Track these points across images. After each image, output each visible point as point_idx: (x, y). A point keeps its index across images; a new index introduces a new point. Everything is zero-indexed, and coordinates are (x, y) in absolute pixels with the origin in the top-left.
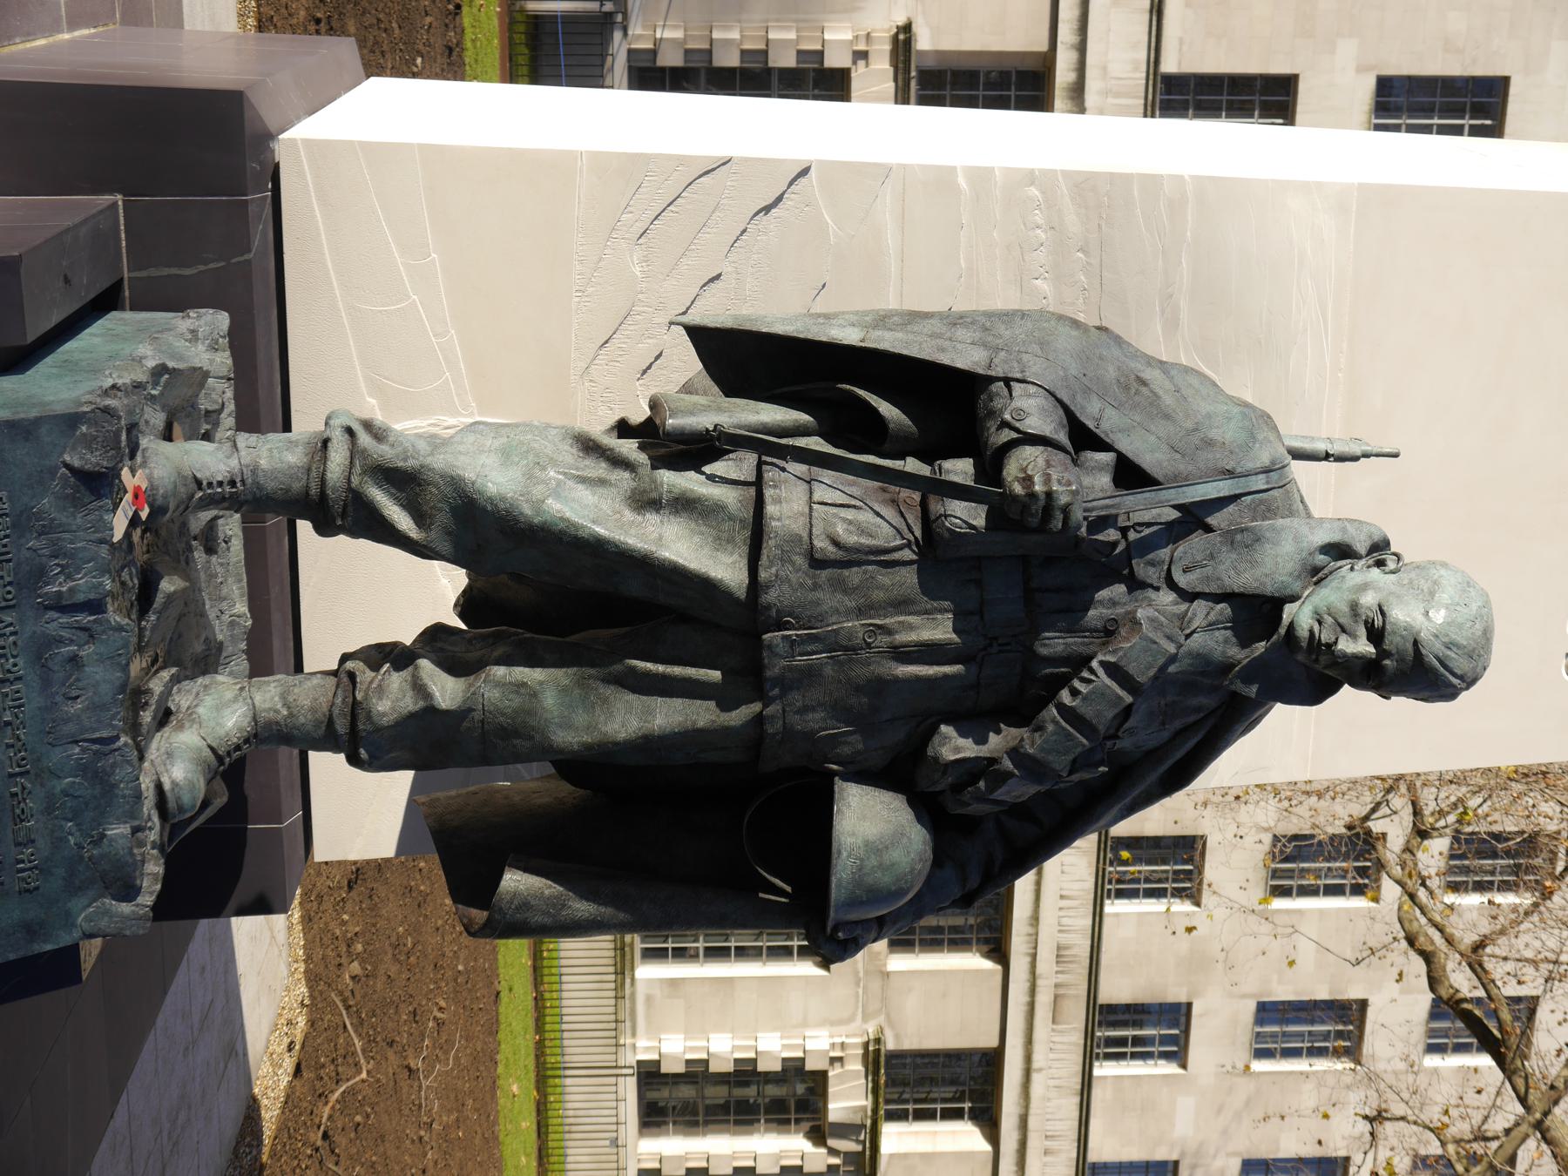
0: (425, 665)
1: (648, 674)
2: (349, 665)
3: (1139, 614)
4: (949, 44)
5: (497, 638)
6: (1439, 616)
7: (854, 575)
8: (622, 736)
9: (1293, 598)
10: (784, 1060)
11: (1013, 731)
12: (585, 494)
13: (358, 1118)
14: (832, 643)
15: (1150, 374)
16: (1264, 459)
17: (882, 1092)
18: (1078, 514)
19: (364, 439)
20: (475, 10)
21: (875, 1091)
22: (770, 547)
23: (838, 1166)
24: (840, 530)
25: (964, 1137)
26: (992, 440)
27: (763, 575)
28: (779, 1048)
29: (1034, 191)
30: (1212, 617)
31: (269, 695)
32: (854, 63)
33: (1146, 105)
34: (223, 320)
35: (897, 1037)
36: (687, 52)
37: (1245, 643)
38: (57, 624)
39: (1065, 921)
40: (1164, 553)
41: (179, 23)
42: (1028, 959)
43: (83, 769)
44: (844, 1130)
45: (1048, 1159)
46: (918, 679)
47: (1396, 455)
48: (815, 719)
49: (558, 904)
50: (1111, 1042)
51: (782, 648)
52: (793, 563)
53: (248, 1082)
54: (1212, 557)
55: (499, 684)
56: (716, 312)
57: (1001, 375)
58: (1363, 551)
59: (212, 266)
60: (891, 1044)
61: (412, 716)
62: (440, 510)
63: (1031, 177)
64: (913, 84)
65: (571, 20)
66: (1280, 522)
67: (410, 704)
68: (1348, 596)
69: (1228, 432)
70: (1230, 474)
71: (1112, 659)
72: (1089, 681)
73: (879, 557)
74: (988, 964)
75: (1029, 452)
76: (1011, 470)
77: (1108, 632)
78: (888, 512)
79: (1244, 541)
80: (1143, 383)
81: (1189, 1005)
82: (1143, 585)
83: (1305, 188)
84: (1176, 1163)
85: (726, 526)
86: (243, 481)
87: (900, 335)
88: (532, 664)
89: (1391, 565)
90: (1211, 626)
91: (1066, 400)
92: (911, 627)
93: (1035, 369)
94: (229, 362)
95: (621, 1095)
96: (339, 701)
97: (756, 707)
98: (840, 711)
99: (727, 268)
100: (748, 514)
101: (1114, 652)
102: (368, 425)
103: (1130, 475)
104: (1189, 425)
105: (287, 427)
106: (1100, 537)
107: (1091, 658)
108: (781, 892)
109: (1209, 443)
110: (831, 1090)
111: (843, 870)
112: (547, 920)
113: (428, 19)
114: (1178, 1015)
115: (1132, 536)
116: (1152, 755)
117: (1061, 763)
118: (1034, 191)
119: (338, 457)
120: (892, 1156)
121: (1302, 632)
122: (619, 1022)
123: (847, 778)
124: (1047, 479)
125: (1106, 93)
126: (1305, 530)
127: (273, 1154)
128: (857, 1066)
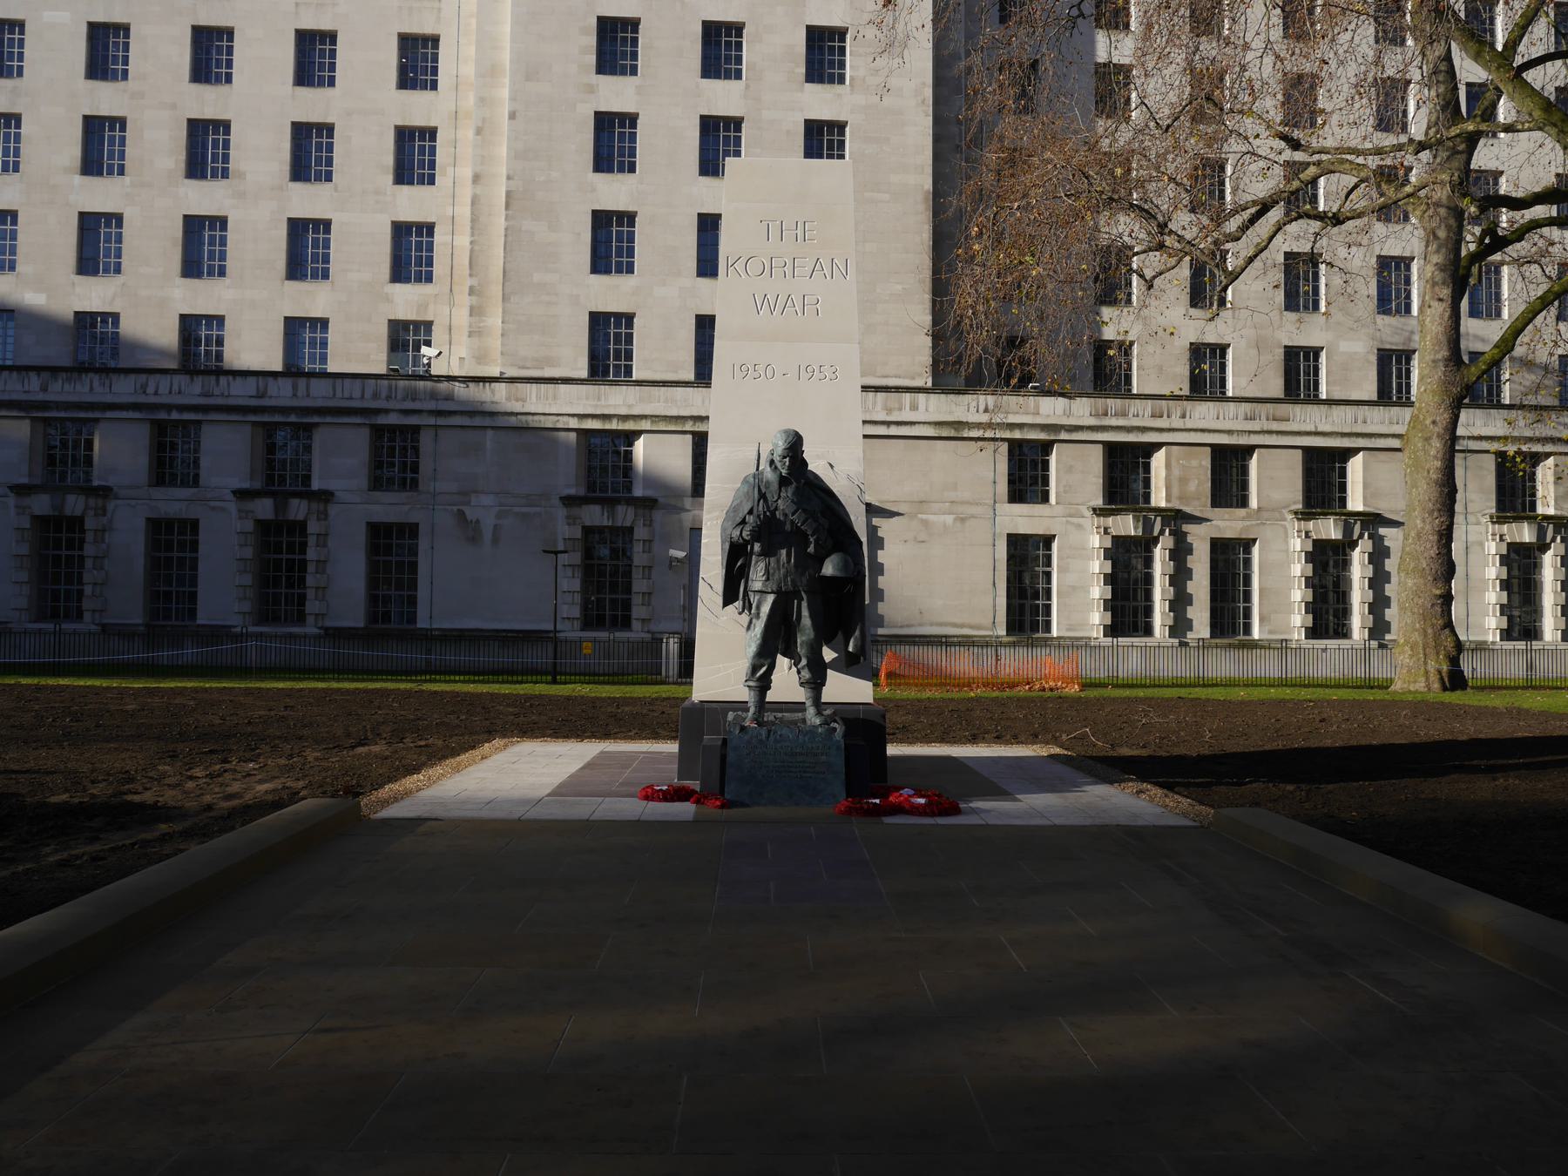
7: (771, 571)
10: (1306, 562)
14: (786, 576)
17: (1326, 511)
21: (1325, 514)
22: (764, 589)
23: (1369, 534)
24: (761, 574)
25: (1355, 468)
28: (1299, 565)
35: (1295, 503)
37: (791, 483)
38: (772, 737)
39: (1231, 416)
40: (770, 503)
42: (1252, 435)
43: (805, 736)
44: (1348, 530)
45: (1368, 421)
48: (804, 580)
49: (855, 639)
50: (1307, 388)
56: (720, 600)
61: (810, 670)
67: (806, 670)
74: (1255, 456)
75: (743, 535)
76: (747, 538)
77: (786, 515)
79: (768, 484)
81: (1285, 347)
84: (1378, 350)
88: (796, 642)
95: (1324, 647)
103: (750, 512)
109: (748, 492)
110: (1324, 537)
111: (838, 574)
114: (1292, 354)
119: (751, 684)
122: (1283, 646)
128: (1311, 525)
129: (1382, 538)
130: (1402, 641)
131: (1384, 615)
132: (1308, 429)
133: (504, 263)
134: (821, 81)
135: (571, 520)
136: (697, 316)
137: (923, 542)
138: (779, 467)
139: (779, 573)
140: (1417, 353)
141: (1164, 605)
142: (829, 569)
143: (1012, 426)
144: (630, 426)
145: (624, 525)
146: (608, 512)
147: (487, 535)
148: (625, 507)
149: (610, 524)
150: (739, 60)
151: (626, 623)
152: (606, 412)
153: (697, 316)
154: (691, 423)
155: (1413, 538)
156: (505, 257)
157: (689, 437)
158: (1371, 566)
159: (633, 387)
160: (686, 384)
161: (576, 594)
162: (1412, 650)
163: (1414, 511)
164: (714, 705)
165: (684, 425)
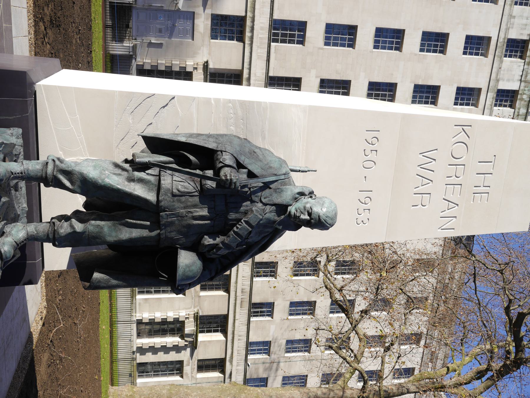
0: (73, 220)
1: (131, 223)
2: (53, 220)
3: (253, 209)
4: (217, 67)
5: (92, 214)
6: (324, 210)
7: (183, 199)
8: (124, 238)
9: (290, 205)
10: (174, 318)
11: (223, 237)
12: (115, 178)
13: (60, 336)
14: (177, 215)
15: (256, 150)
16: (284, 171)
17: (198, 326)
18: (238, 184)
19: (57, 162)
20: (96, 53)
22: (162, 191)
24: (180, 187)
25: (219, 336)
26: (217, 166)
27: (160, 198)
28: (173, 315)
29: (230, 105)
30: (271, 209)
31: (32, 228)
32: (194, 70)
33: (265, 83)
34: (20, 131)
35: (202, 312)
36: (152, 66)
37: (279, 216)
39: (244, 283)
40: (259, 194)
41: (12, 53)
42: (235, 292)
44: (189, 335)
45: (239, 341)
46: (199, 224)
47: (316, 171)
48: (173, 234)
50: (255, 312)
51: (165, 217)
52: (168, 196)
53: (30, 328)
54: (271, 195)
55: (92, 225)
56: (150, 132)
57: (220, 150)
58: (307, 194)
59: (17, 116)
60: (201, 314)
61: (70, 233)
62: (77, 181)
63: (230, 101)
64: (208, 76)
65: (121, 56)
66: (287, 187)
67: (69, 230)
68: (303, 205)
69: (275, 165)
70: (276, 175)
71: (246, 220)
72: (241, 225)
73: (189, 194)
74: (225, 294)
75: (226, 169)
76: (222, 173)
77: (246, 213)
78: (192, 183)
79: (279, 191)
80: (255, 152)
82: (254, 202)
83: (296, 106)
84: (271, 341)
85: (151, 186)
86: (24, 173)
87: (195, 139)
88: (101, 220)
89: (314, 197)
90: (271, 212)
91: (236, 156)
92: (197, 212)
93: (229, 148)
94: (22, 141)
96: (50, 229)
97: (158, 231)
98: (179, 232)
99: (153, 121)
100: (157, 183)
101: (247, 218)
102: (59, 159)
103: (251, 175)
104: (266, 163)
105: (38, 159)
106: (243, 190)
107: (241, 219)
108: (165, 277)
109: (271, 167)
111: (180, 271)
112: (105, 285)
113: (83, 54)
115: (252, 190)
116: (257, 243)
117: (234, 245)
118: (230, 105)
120: (201, 341)
121: (293, 214)
122: (132, 310)
123: (181, 249)
124: (231, 176)
125: (256, 80)
126: (293, 189)
127: (36, 346)
128: (192, 319)
129: (185, 349)
130: (135, 390)
131: (149, 352)
132: (236, 316)
134: (414, 91)
136: (306, 22)
139: (182, 208)
140: (268, 357)
141: (152, 344)
150: (428, 51)
153: (306, 22)
155: (187, 392)
157: (243, 14)
158: (172, 346)
160: (272, 14)
162: (130, 396)
163: (200, 391)
164: (31, 108)
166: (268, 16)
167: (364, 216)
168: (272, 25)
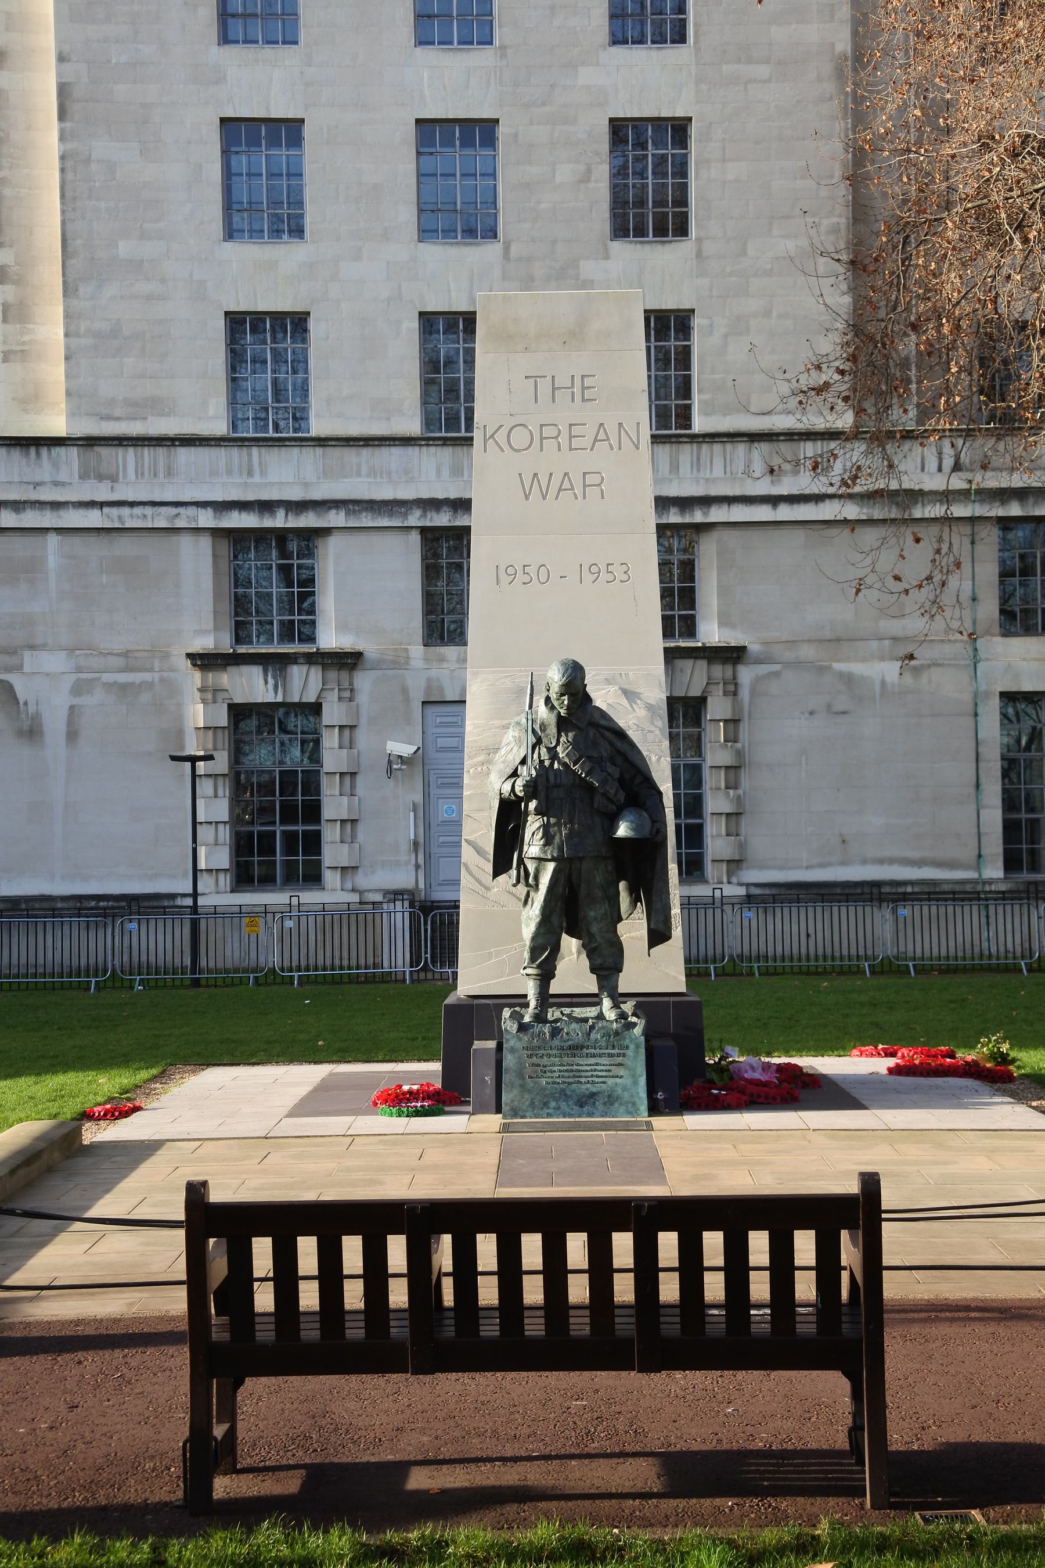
22: (542, 856)
56: (489, 868)
76: (521, 794)
79: (543, 727)
90: (567, 736)
103: (523, 762)
116: (611, 744)
133: (63, 223)
135: (210, 694)
137: (844, 713)
138: (556, 704)
142: (623, 830)
143: (1003, 495)
144: (308, 520)
145: (304, 700)
146: (274, 677)
147: (55, 724)
148: (305, 668)
149: (280, 699)
151: (313, 878)
152: (265, 496)
154: (418, 513)
156: (63, 212)
157: (415, 538)
159: (311, 449)
160: (406, 441)
161: (221, 827)
165: (405, 516)
166: (413, 452)
167: (618, 572)
168: (443, 434)
